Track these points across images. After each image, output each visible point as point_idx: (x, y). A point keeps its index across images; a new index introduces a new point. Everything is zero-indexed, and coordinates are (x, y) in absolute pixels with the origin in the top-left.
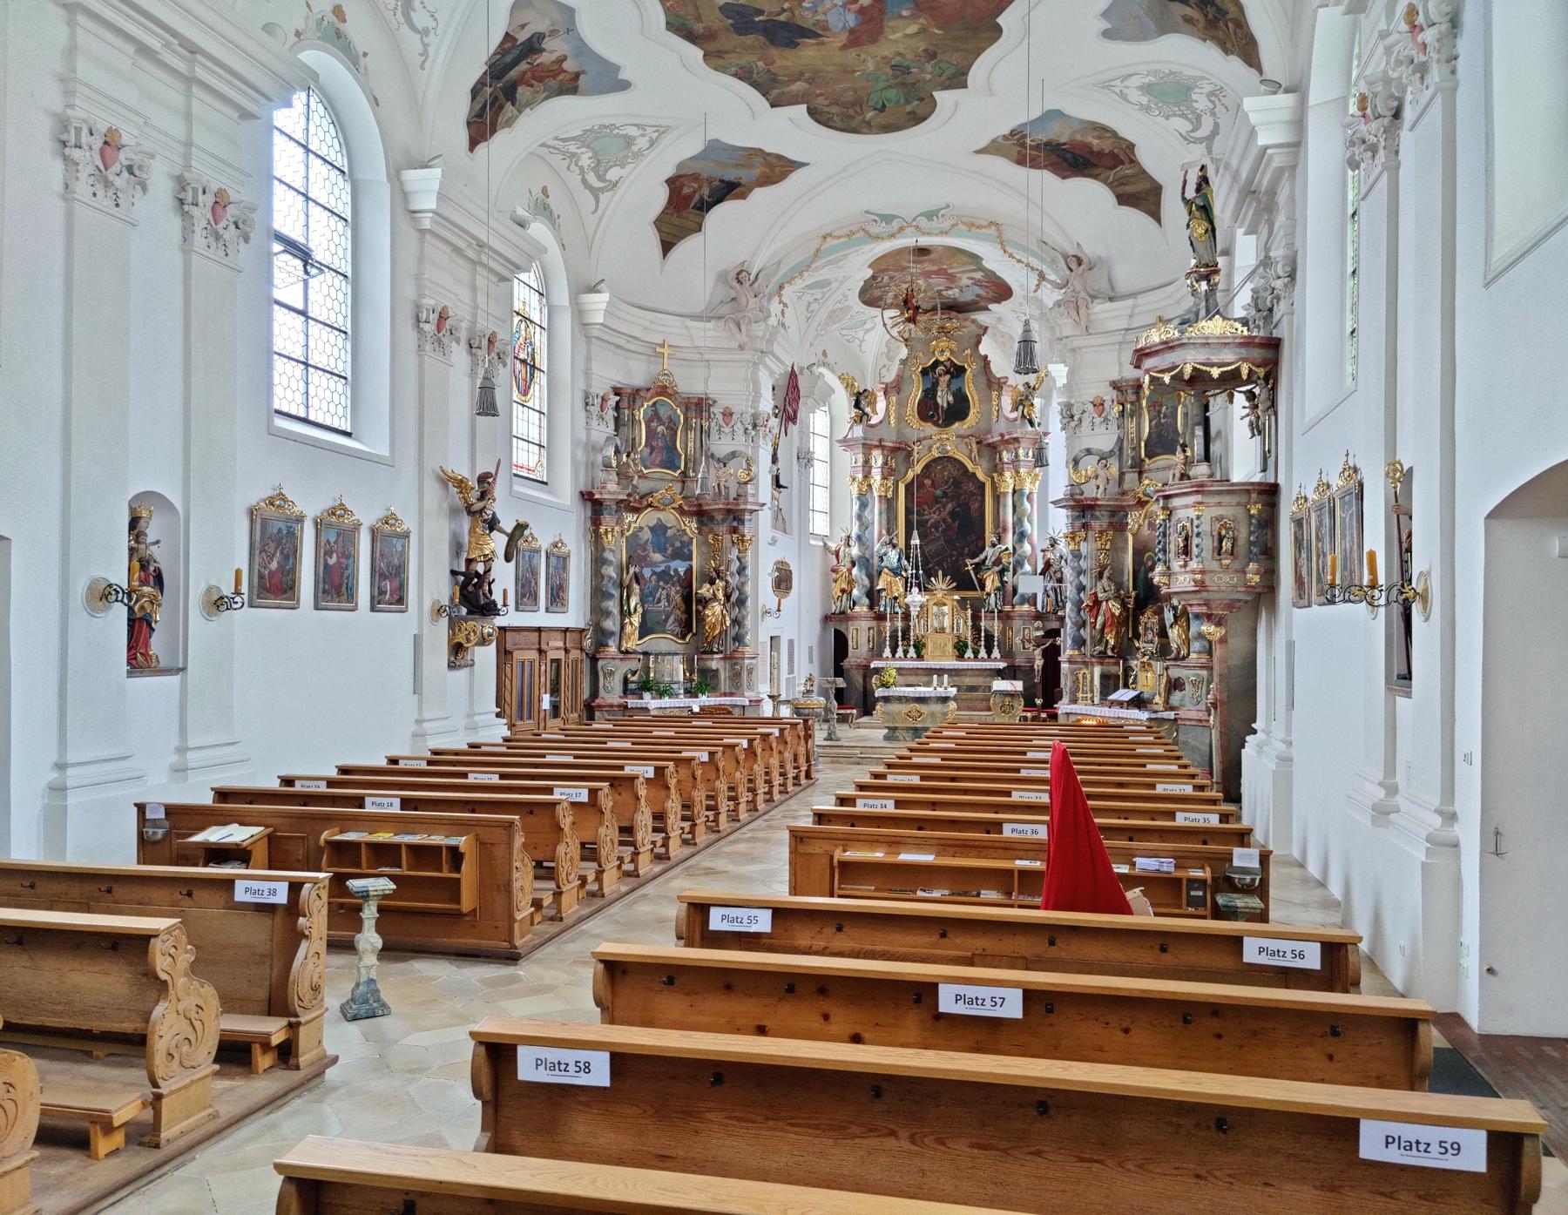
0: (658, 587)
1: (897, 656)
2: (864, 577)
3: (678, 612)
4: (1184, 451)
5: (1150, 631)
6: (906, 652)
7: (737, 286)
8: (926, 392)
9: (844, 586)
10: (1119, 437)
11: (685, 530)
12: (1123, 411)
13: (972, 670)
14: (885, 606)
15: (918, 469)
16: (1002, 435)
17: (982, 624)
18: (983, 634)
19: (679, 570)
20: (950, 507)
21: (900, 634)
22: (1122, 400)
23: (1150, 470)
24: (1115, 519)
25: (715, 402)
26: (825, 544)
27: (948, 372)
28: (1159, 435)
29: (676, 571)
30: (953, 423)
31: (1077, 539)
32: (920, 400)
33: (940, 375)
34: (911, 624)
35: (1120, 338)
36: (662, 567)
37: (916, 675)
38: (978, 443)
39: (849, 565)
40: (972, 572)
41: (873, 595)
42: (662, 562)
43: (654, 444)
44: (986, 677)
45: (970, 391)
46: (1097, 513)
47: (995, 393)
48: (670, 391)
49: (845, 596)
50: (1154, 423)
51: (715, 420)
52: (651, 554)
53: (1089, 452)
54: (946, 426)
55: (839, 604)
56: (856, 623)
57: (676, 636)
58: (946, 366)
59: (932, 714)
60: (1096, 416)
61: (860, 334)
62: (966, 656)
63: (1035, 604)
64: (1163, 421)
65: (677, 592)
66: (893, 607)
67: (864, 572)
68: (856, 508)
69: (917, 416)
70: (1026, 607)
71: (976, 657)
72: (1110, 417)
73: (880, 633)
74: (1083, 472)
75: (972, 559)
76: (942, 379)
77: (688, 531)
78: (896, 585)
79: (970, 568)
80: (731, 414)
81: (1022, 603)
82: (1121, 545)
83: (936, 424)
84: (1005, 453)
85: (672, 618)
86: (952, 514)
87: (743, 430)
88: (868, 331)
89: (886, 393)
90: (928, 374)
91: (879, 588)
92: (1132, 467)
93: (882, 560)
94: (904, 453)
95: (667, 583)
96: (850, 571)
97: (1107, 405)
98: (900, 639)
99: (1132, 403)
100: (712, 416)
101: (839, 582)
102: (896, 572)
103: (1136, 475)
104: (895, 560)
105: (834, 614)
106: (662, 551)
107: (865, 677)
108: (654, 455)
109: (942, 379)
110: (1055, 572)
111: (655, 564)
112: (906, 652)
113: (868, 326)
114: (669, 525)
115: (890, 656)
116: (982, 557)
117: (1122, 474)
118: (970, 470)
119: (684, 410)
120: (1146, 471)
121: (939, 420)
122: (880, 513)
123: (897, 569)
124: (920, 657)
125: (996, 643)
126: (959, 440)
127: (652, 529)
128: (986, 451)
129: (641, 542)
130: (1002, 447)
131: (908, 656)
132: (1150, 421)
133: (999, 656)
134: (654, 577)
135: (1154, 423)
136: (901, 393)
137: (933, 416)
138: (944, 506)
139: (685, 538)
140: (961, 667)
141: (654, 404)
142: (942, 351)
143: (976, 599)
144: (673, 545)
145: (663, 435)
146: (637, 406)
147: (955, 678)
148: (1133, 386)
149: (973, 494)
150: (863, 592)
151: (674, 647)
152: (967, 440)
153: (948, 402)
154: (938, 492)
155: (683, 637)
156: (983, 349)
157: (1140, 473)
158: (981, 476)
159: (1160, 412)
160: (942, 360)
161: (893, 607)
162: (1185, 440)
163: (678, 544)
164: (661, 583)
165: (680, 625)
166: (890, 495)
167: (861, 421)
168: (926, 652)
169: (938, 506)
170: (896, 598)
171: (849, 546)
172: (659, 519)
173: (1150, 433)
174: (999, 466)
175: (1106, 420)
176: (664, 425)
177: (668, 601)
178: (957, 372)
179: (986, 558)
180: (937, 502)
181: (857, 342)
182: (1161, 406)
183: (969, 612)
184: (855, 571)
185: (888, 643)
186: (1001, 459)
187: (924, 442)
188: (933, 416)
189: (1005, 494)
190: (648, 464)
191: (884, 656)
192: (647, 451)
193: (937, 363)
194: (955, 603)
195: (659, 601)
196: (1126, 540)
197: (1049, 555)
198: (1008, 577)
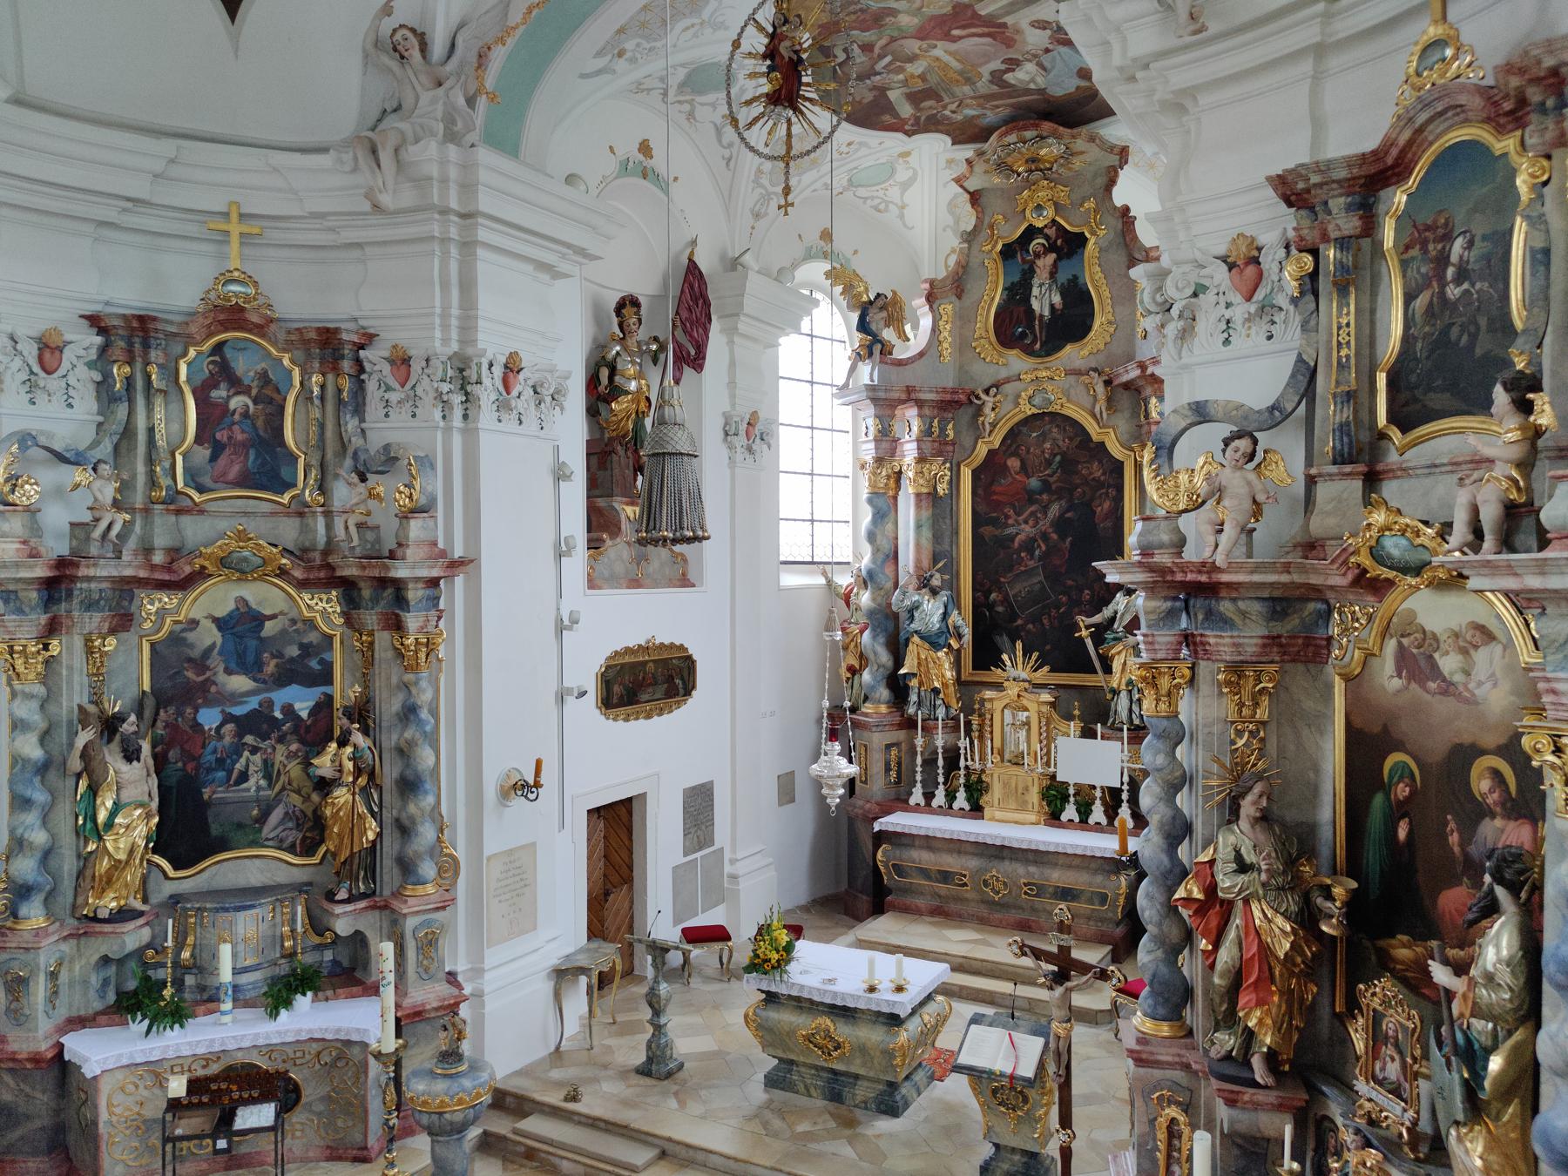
3: (295, 799)
4: (1525, 407)
5: (1389, 1050)
6: (950, 796)
7: (394, 65)
8: (1011, 290)
10: (1300, 360)
12: (1314, 275)
16: (1142, 366)
19: (297, 706)
20: (1054, 510)
22: (1311, 236)
23: (1405, 472)
24: (1291, 625)
26: (830, 583)
27: (1051, 248)
28: (1441, 342)
29: (289, 710)
30: (1059, 348)
31: (1165, 682)
33: (1037, 256)
35: (1308, 35)
36: (253, 703)
37: (959, 852)
40: (1089, 642)
41: (898, 688)
43: (221, 436)
45: (1094, 277)
46: (1225, 607)
48: (255, 318)
50: (1420, 303)
52: (222, 677)
53: (1201, 413)
54: (1048, 355)
57: (291, 849)
58: (1047, 238)
59: (863, 1050)
60: (1237, 298)
61: (894, 193)
62: (1064, 817)
64: (1453, 292)
67: (882, 640)
69: (993, 338)
71: (1084, 820)
72: (1282, 301)
74: (1183, 478)
76: (1040, 263)
82: (1309, 704)
83: (1029, 351)
84: (1154, 400)
85: (276, 816)
86: (1061, 525)
88: (905, 186)
89: (931, 298)
90: (1013, 256)
92: (1339, 459)
93: (912, 618)
94: (970, 410)
97: (1269, 262)
99: (1343, 243)
102: (934, 641)
103: (1357, 485)
106: (244, 663)
108: (223, 460)
109: (1040, 263)
111: (235, 698)
112: (950, 796)
113: (902, 175)
114: (267, 612)
116: (1107, 612)
117: (1311, 481)
118: (1095, 438)
120: (1391, 473)
121: (1034, 342)
123: (940, 633)
124: (976, 810)
126: (1072, 379)
127: (221, 623)
128: (1124, 399)
131: (956, 805)
132: (1409, 298)
134: (230, 727)
135: (1420, 303)
136: (965, 297)
137: (1023, 335)
138: (1045, 509)
139: (312, 637)
141: (218, 348)
142: (1039, 208)
144: (280, 655)
145: (246, 415)
147: (1032, 869)
148: (1348, 185)
149: (1100, 484)
151: (283, 875)
153: (1052, 306)
154: (1034, 483)
156: (1120, 196)
157: (1372, 480)
158: (1116, 450)
159: (1443, 260)
160: (1039, 224)
162: (1535, 362)
163: (293, 651)
164: (249, 739)
165: (298, 826)
166: (942, 489)
167: (871, 354)
168: (989, 800)
169: (1033, 508)
170: (936, 691)
172: (241, 600)
173: (1407, 339)
174: (1145, 429)
175: (1267, 310)
176: (246, 391)
177: (268, 776)
178: (1070, 245)
180: (1031, 501)
181: (893, 209)
182: (1448, 238)
185: (919, 777)
186: (1147, 416)
187: (1007, 388)
188: (1023, 335)
190: (206, 481)
191: (912, 801)
192: (204, 453)
193: (1031, 232)
194: (1045, 709)
195: (244, 777)
196: (1329, 687)
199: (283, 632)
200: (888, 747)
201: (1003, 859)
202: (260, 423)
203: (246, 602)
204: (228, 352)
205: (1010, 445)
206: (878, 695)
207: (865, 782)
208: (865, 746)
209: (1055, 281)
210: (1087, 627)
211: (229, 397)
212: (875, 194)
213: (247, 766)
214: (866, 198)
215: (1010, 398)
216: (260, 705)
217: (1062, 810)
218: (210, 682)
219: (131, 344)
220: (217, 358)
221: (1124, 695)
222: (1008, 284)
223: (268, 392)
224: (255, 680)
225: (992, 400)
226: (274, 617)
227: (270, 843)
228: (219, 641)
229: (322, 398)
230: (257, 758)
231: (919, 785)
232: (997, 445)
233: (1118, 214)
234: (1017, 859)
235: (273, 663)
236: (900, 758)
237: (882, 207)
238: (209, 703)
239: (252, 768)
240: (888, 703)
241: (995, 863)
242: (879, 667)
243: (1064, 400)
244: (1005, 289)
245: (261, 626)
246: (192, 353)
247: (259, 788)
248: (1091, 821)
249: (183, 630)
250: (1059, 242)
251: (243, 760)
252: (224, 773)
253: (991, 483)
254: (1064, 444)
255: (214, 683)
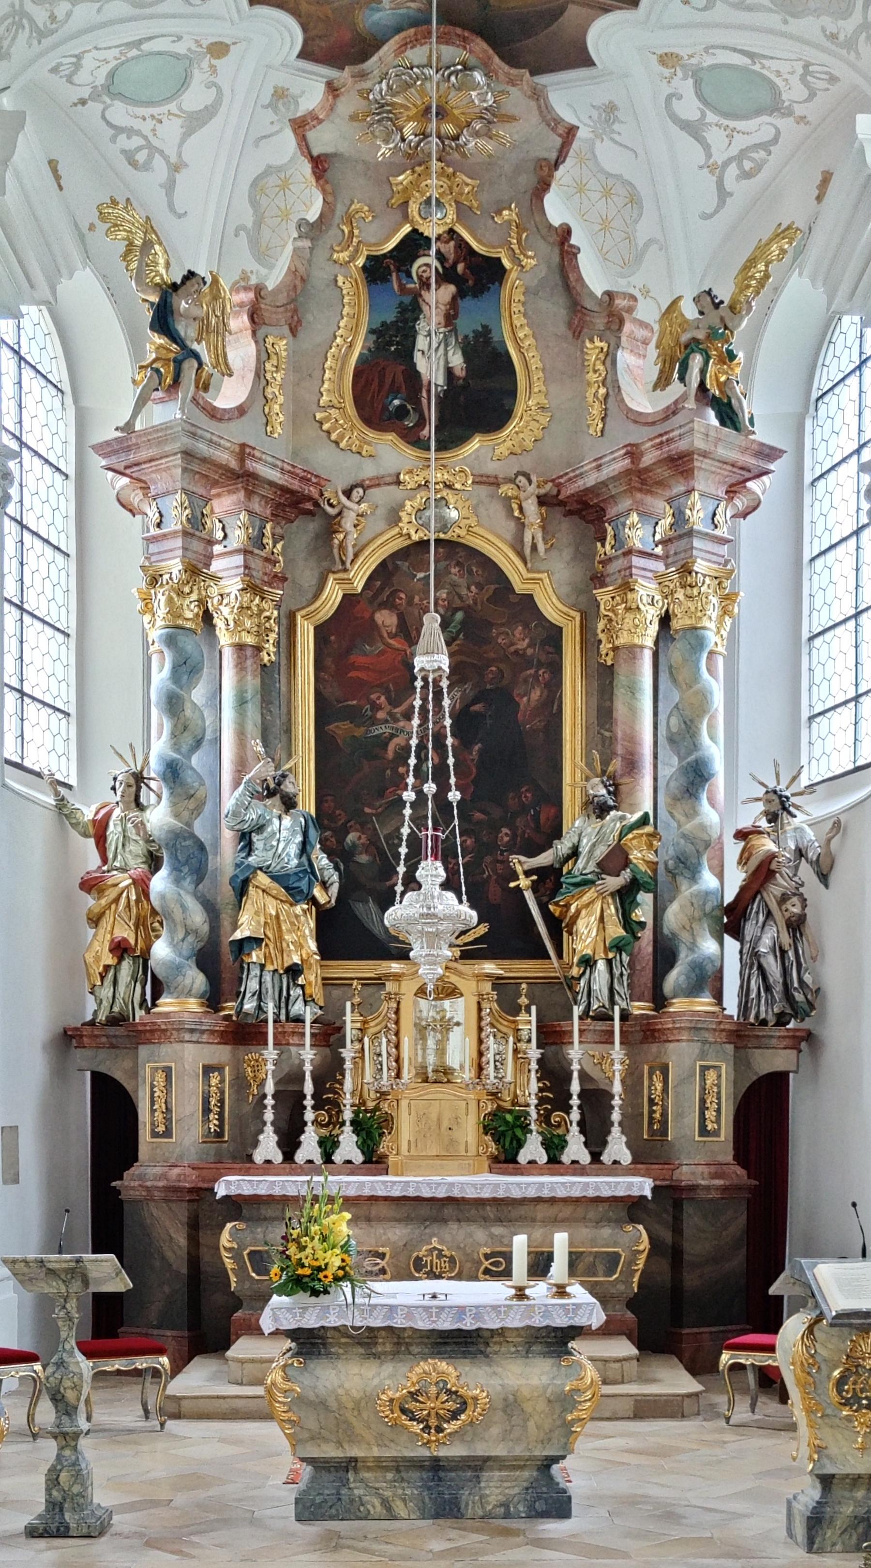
1: (300, 1156)
2: (191, 903)
6: (328, 1146)
9: (125, 932)
13: (553, 1200)
14: (260, 995)
15: (359, 580)
17: (575, 1053)
18: (575, 1087)
21: (309, 1087)
26: (61, 804)
27: (447, 276)
30: (461, 440)
32: (362, 359)
34: (348, 1053)
38: (542, 501)
39: (138, 867)
40: (529, 896)
44: (598, 1223)
47: (594, 347)
49: (126, 967)
55: (106, 992)
56: (166, 1049)
62: (523, 1157)
63: (718, 996)
66: (283, 1001)
68: (161, 676)
69: (351, 410)
70: (704, 1003)
71: (554, 1159)
73: (241, 1083)
75: (531, 855)
78: (295, 928)
79: (524, 882)
81: (694, 989)
91: (238, 935)
93: (249, 848)
96: (142, 885)
98: (309, 1102)
101: (106, 923)
104: (293, 849)
105: (92, 1023)
107: (194, 1226)
110: (783, 899)
112: (328, 1146)
115: (277, 1157)
122: (241, 702)
123: (299, 874)
125: (616, 1116)
126: (483, 491)
128: (565, 528)
130: (626, 503)
131: (338, 1157)
133: (626, 1157)
136: (301, 334)
137: (401, 412)
140: (516, 1194)
143: (550, 983)
150: (186, 948)
152: (507, 490)
153: (449, 372)
161: (283, 1001)
170: (294, 971)
171: (139, 806)
179: (575, 853)
183: (529, 1022)
184: (160, 883)
185: (269, 1116)
187: (377, 494)
188: (401, 412)
189: (633, 650)
191: (259, 1156)
194: (487, 987)
197: (768, 845)
198: (643, 912)
200: (208, 1070)
201: (444, 1221)
205: (382, 589)
206: (188, 981)
207: (168, 1133)
208: (168, 1071)
209: (455, 331)
210: (527, 874)
212: (137, 124)
214: (119, 130)
215: (381, 512)
217: (520, 1144)
221: (601, 965)
222: (376, 325)
225: (355, 507)
231: (269, 1129)
232: (359, 585)
233: (554, 238)
234: (468, 1220)
236: (222, 1092)
237: (141, 157)
240: (202, 996)
241: (435, 1228)
242: (187, 933)
243: (473, 521)
244: (371, 331)
248: (566, 1158)
250: (460, 267)
253: (349, 651)
254: (470, 594)
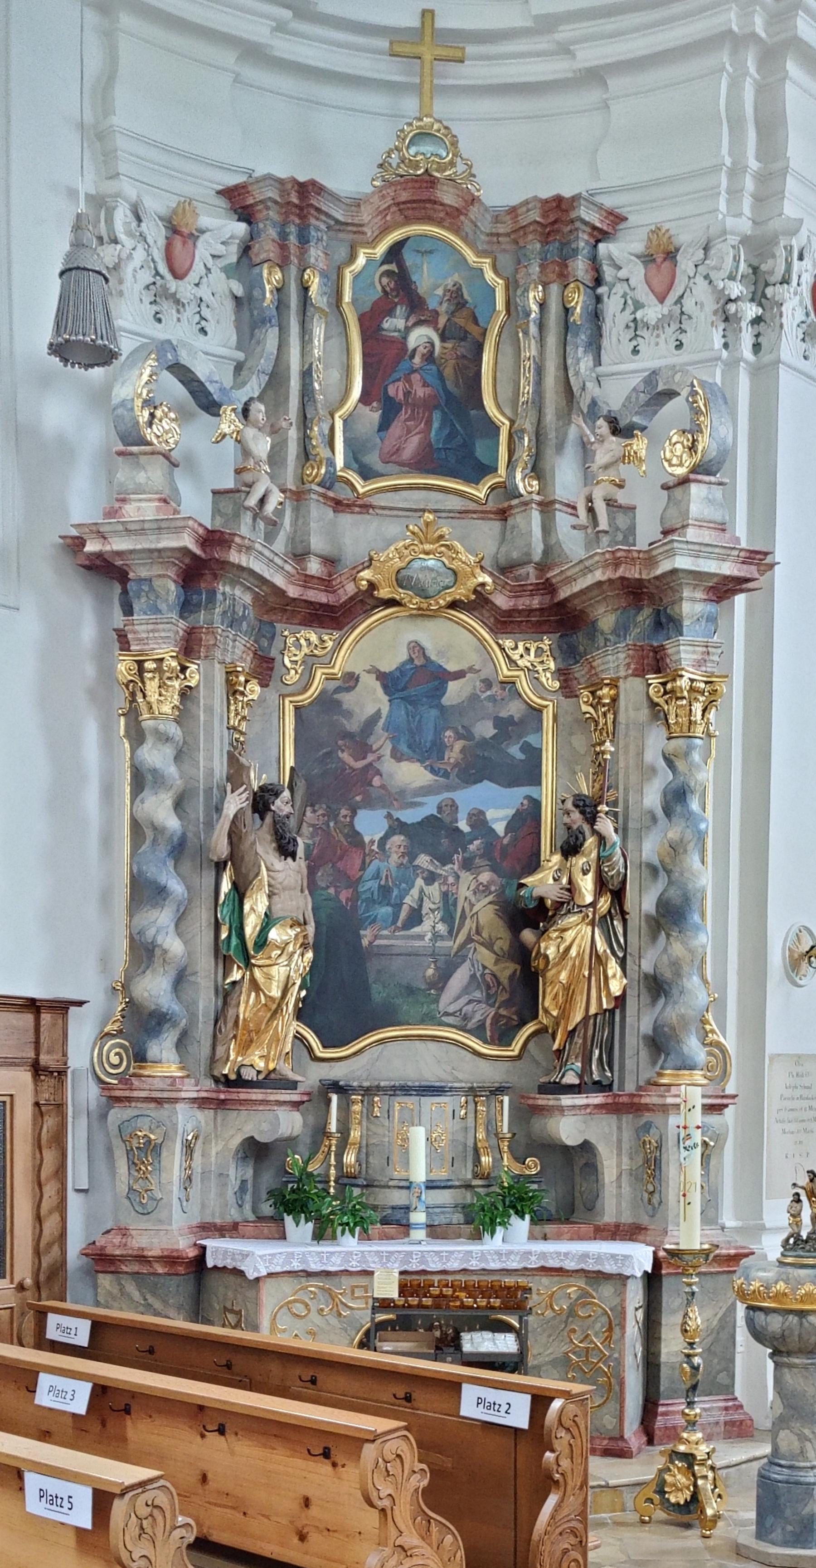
0: (409, 869)
3: (485, 956)
11: (509, 684)
19: (490, 814)
25: (616, 218)
29: (478, 820)
36: (429, 807)
42: (427, 791)
43: (396, 390)
48: (448, 197)
51: (620, 289)
52: (388, 765)
57: (478, 1032)
65: (482, 890)
77: (524, 685)
80: (671, 255)
85: (459, 978)
87: (711, 305)
95: (445, 860)
100: (608, 273)
108: (396, 428)
114: (451, 667)
119: (506, 260)
127: (390, 682)
129: (353, 726)
134: (398, 839)
139: (514, 709)
141: (395, 252)
144: (466, 735)
145: (429, 357)
146: (315, 253)
155: (503, 1037)
163: (486, 730)
164: (423, 860)
165: (490, 999)
172: (417, 647)
176: (431, 320)
177: (448, 918)
190: (373, 459)
192: (372, 416)
195: (416, 917)
199: (474, 698)
202: (448, 372)
203: (422, 650)
204: (409, 258)
211: (408, 330)
213: (421, 900)
216: (440, 809)
218: (371, 770)
219: (283, 235)
220: (393, 267)
223: (460, 321)
224: (433, 771)
226: (459, 675)
227: (450, 1020)
228: (385, 710)
229: (541, 326)
230: (434, 891)
235: (458, 745)
238: (369, 803)
239: (427, 905)
245: (441, 690)
246: (361, 261)
247: (436, 936)
249: (338, 690)
251: (415, 892)
252: (389, 909)
255: (379, 773)
